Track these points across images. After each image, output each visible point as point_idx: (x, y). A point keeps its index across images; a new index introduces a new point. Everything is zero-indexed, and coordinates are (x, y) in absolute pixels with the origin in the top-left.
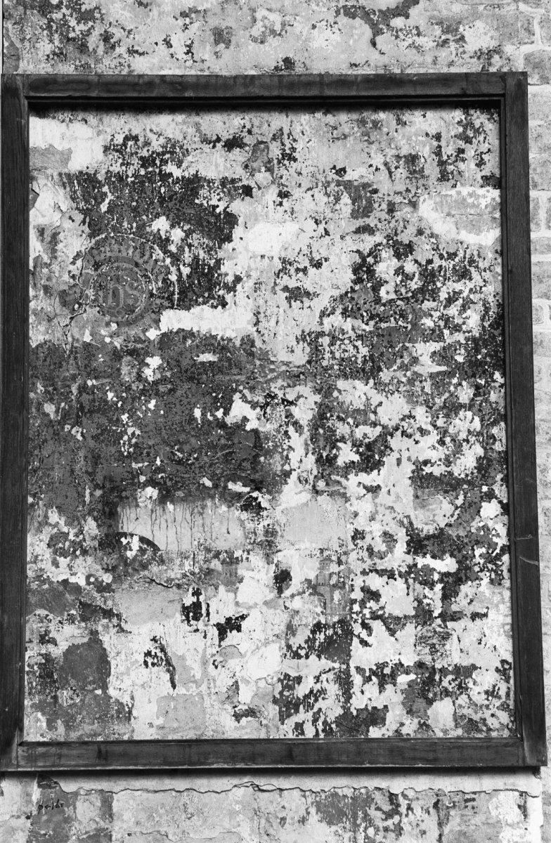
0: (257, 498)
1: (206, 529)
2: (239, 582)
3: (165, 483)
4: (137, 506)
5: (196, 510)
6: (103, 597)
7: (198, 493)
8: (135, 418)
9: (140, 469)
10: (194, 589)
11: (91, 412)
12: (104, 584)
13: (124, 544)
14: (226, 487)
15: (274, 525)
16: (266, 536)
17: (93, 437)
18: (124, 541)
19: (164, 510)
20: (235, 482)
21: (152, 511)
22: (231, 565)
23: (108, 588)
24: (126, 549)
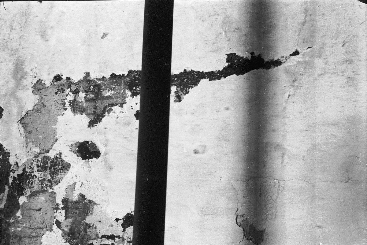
0: (14, 178)
1: (34, 234)
2: (85, 199)
15: (38, 160)
22: (68, 208)
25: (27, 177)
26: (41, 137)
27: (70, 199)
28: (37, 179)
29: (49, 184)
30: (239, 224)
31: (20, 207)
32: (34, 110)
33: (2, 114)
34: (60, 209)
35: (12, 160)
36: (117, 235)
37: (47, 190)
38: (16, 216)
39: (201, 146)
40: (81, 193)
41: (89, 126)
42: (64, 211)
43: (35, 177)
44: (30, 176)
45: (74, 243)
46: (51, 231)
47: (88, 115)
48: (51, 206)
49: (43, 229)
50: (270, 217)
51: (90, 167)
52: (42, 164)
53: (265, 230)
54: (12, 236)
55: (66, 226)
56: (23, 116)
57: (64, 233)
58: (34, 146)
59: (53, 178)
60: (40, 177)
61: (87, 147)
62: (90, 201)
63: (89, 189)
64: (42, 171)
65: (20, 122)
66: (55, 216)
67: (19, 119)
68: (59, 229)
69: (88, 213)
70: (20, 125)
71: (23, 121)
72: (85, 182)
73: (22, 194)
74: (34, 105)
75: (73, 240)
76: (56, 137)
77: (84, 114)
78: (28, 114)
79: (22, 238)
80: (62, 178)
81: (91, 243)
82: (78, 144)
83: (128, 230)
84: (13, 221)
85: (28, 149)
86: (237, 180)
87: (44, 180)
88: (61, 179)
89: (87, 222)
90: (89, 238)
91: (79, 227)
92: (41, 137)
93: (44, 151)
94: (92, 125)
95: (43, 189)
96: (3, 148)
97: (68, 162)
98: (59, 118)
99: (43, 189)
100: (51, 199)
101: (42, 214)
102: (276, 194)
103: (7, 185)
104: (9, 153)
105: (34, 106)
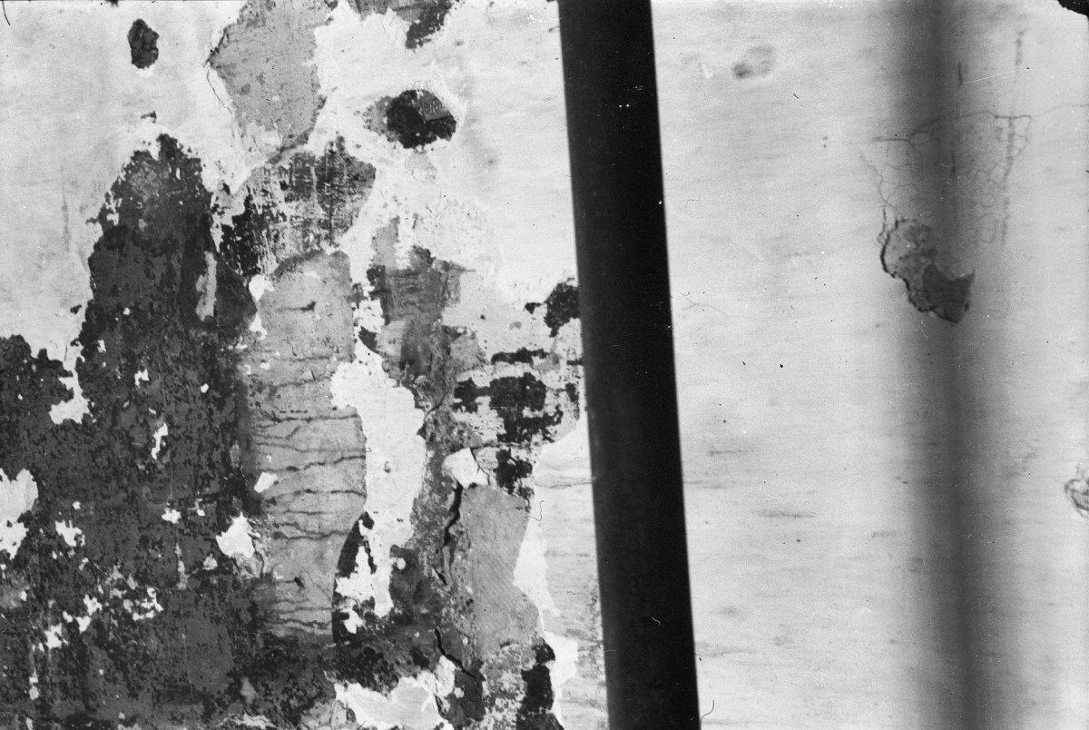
0: (225, 228)
1: (308, 375)
2: (431, 260)
3: (214, 497)
4: (267, 578)
5: (267, 408)
6: (493, 703)
7: (230, 405)
8: (88, 576)
9: (189, 571)
10: (456, 407)
11: (86, 696)
12: (459, 693)
13: (361, 622)
14: (209, 324)
15: (282, 170)
16: (310, 189)
17: (133, 695)
18: (353, 624)
19: (273, 501)
20: (194, 298)
21: (277, 536)
23: (470, 678)
24: (370, 618)
25: (261, 222)
26: (276, 98)
27: (388, 265)
28: (288, 223)
29: (324, 232)
30: (892, 270)
31: (258, 307)
32: (245, 23)
33: (157, 50)
34: (367, 298)
35: (210, 179)
36: (536, 349)
37: (322, 250)
38: (251, 333)
39: (753, 51)
40: (418, 245)
41: (410, 44)
42: (377, 303)
43: (281, 218)
44: (268, 217)
45: (419, 385)
46: (351, 361)
47: (399, 10)
48: (340, 293)
49: (328, 358)
50: (986, 235)
51: (432, 168)
52: (294, 179)
53: (973, 275)
54: (251, 386)
55: (390, 343)
56: (215, 45)
57: (387, 361)
58: (263, 127)
59: (331, 215)
60: (297, 217)
61: (414, 111)
62: (446, 266)
63: (437, 231)
64: (298, 199)
65: (212, 64)
66: (357, 320)
67: (207, 54)
68: (372, 353)
69: (445, 299)
70: (214, 74)
71: (218, 60)
72: (422, 212)
73: (256, 271)
74: (241, 7)
75: (415, 378)
76: (320, 92)
77: (389, 10)
78: (228, 36)
79: (277, 387)
80: (358, 210)
81: (467, 379)
82: (386, 104)
83: (563, 330)
84: (245, 346)
85: (248, 141)
86: (878, 139)
87: (307, 223)
88: (355, 213)
89: (447, 325)
90: (460, 368)
91: (426, 340)
92: (276, 98)
93: (294, 139)
94: (417, 41)
95: (309, 250)
96: (178, 147)
97: (366, 162)
98: (320, 34)
99: (309, 250)
100: (337, 274)
101: (318, 317)
102: (1003, 164)
103: (210, 251)
104: (198, 161)
105: (242, 10)
